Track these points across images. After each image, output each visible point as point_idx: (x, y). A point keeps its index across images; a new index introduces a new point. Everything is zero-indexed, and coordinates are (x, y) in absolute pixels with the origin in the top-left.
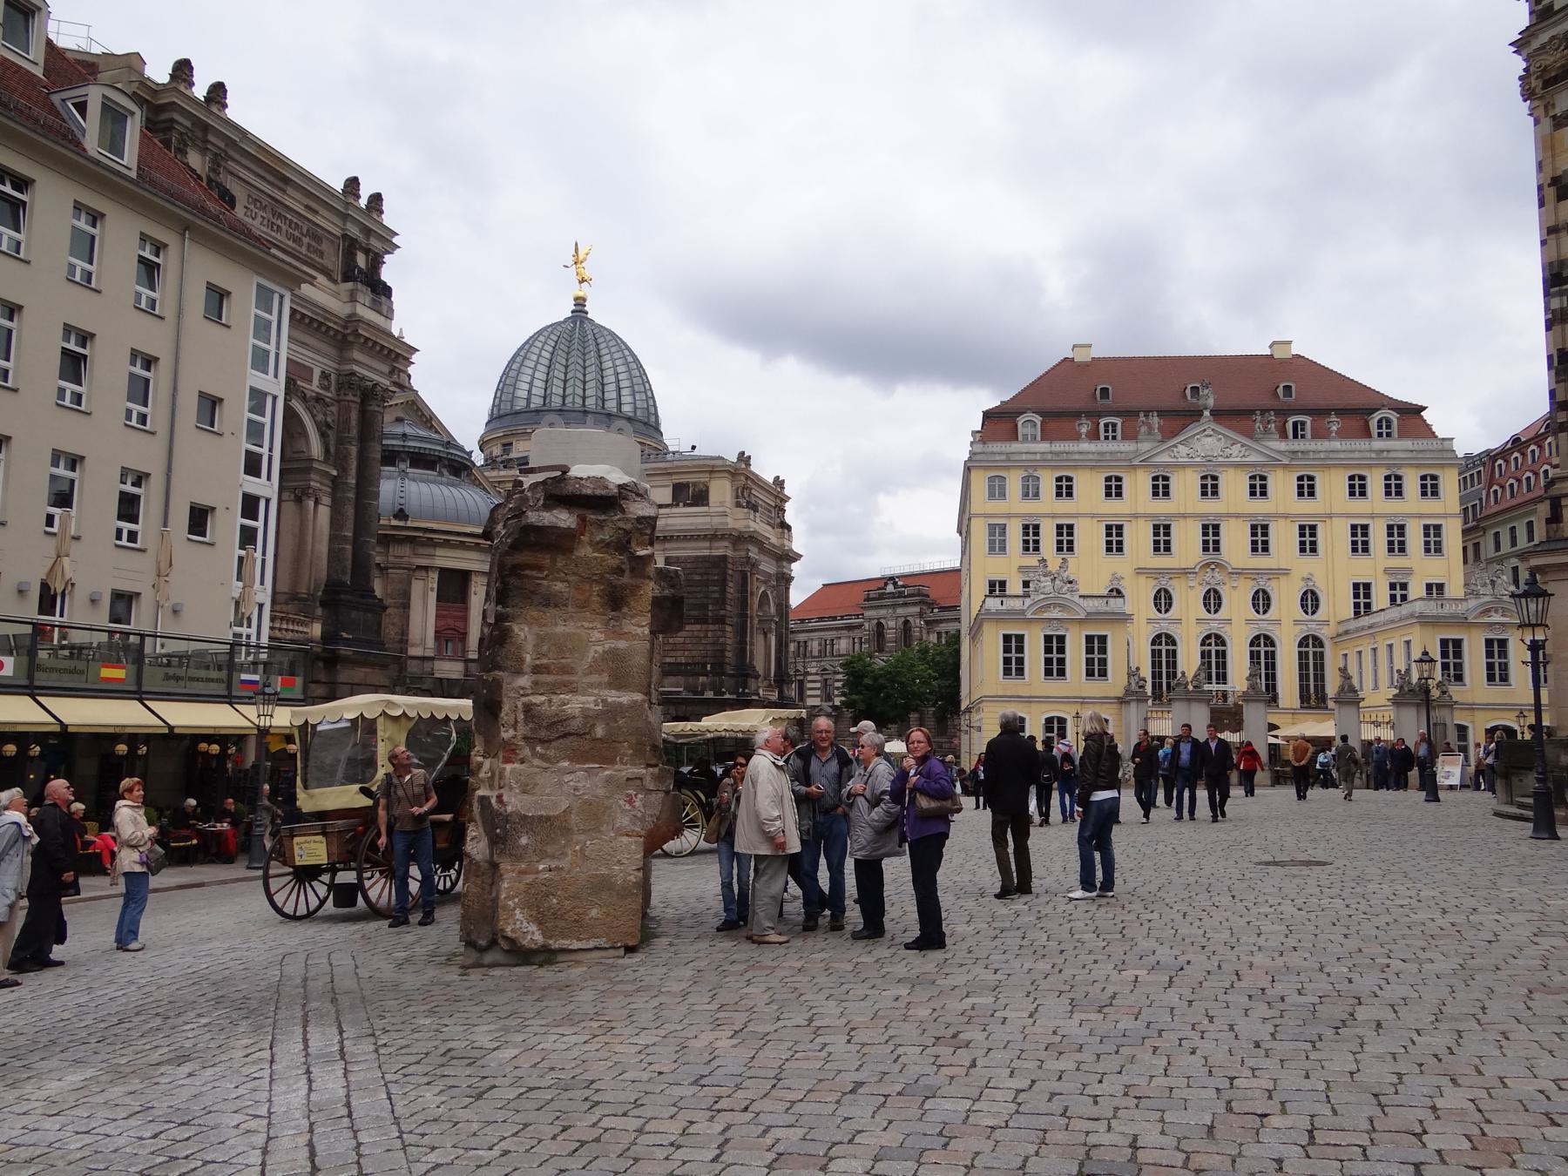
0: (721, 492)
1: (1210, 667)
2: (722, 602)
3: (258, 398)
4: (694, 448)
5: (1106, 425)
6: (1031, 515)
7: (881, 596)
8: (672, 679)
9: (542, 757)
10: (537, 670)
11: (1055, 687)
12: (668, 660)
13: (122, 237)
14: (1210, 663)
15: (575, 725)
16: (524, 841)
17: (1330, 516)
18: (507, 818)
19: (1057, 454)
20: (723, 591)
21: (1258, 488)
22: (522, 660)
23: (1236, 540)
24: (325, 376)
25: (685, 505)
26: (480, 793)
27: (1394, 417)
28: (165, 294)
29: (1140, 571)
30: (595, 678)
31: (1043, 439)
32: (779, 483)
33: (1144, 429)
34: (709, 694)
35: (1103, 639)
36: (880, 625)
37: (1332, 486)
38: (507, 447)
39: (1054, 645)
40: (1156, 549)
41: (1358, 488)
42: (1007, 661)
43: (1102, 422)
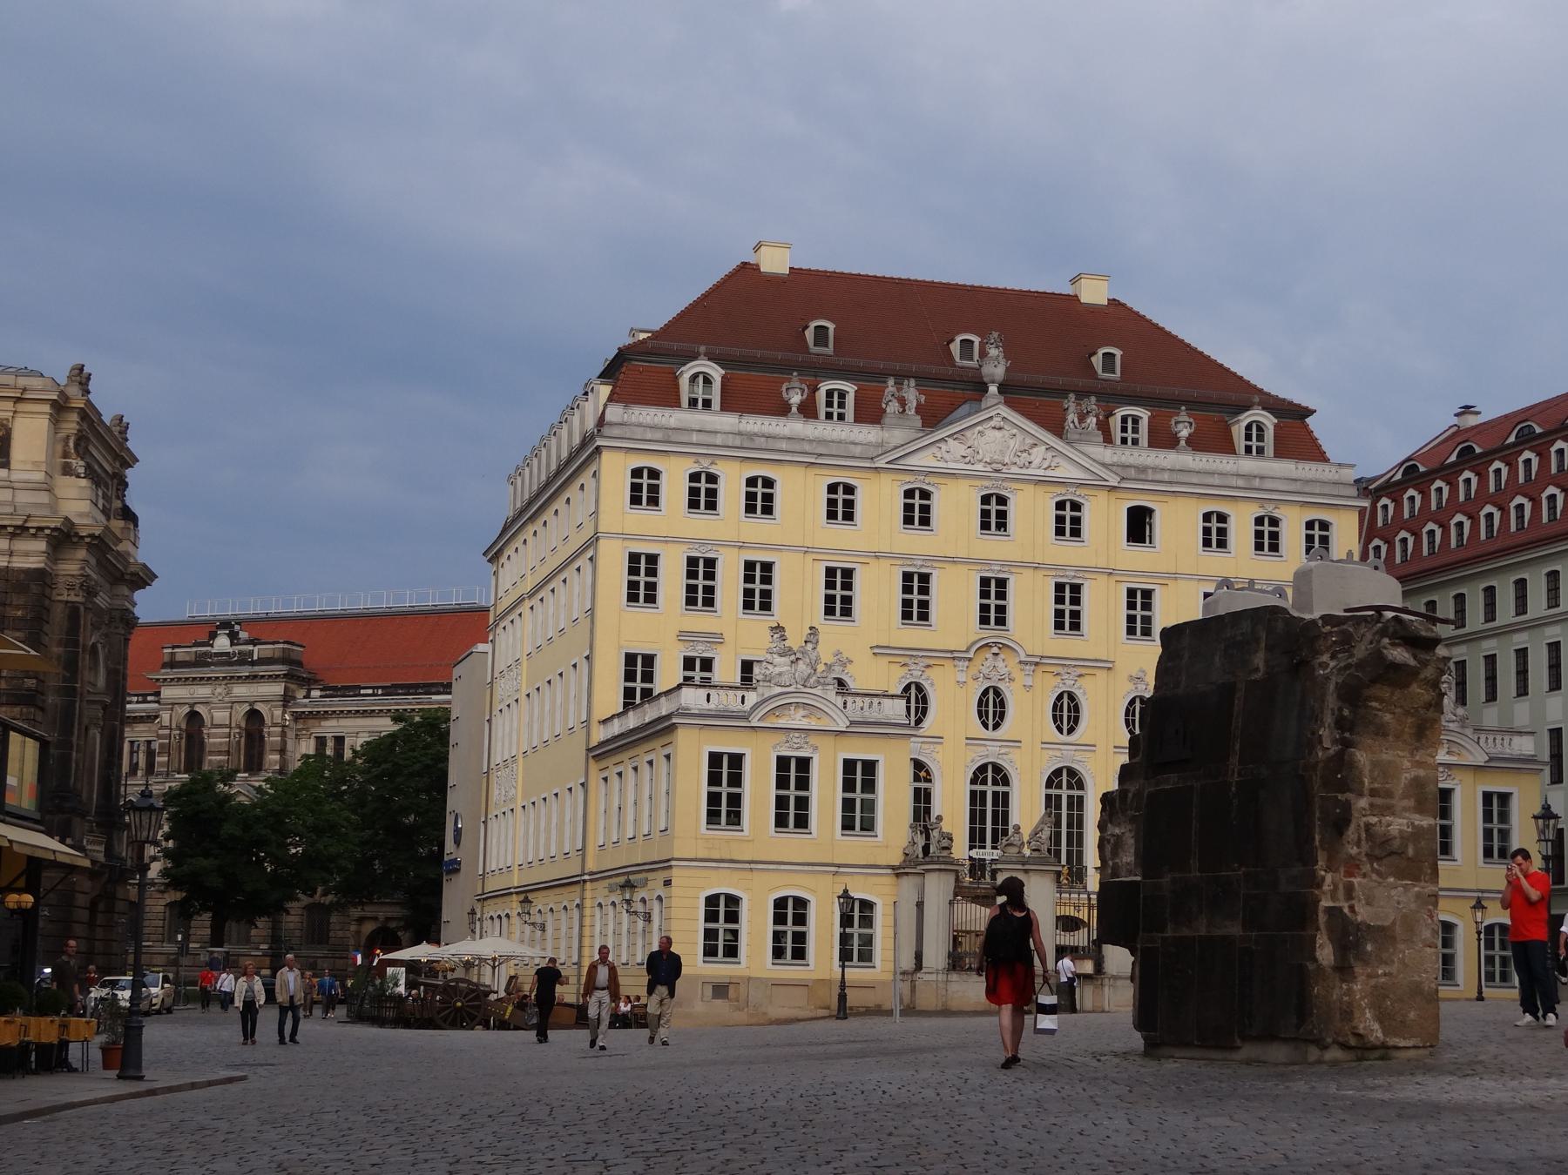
1: (1058, 824)
5: (830, 394)
6: (702, 542)
7: (200, 661)
9: (1379, 873)
10: (1374, 793)
11: (791, 844)
14: (1058, 817)
15: (1396, 843)
16: (1369, 948)
17: (1175, 576)
18: (1358, 926)
19: (751, 436)
21: (1068, 523)
22: (1362, 783)
23: (1030, 605)
26: (1325, 903)
27: (1269, 421)
29: (879, 651)
30: (1406, 803)
31: (726, 407)
32: (122, 425)
33: (893, 407)
35: (870, 767)
36: (194, 717)
37: (1177, 523)
39: (791, 773)
40: (907, 615)
41: (1215, 534)
42: (714, 799)
43: (825, 387)
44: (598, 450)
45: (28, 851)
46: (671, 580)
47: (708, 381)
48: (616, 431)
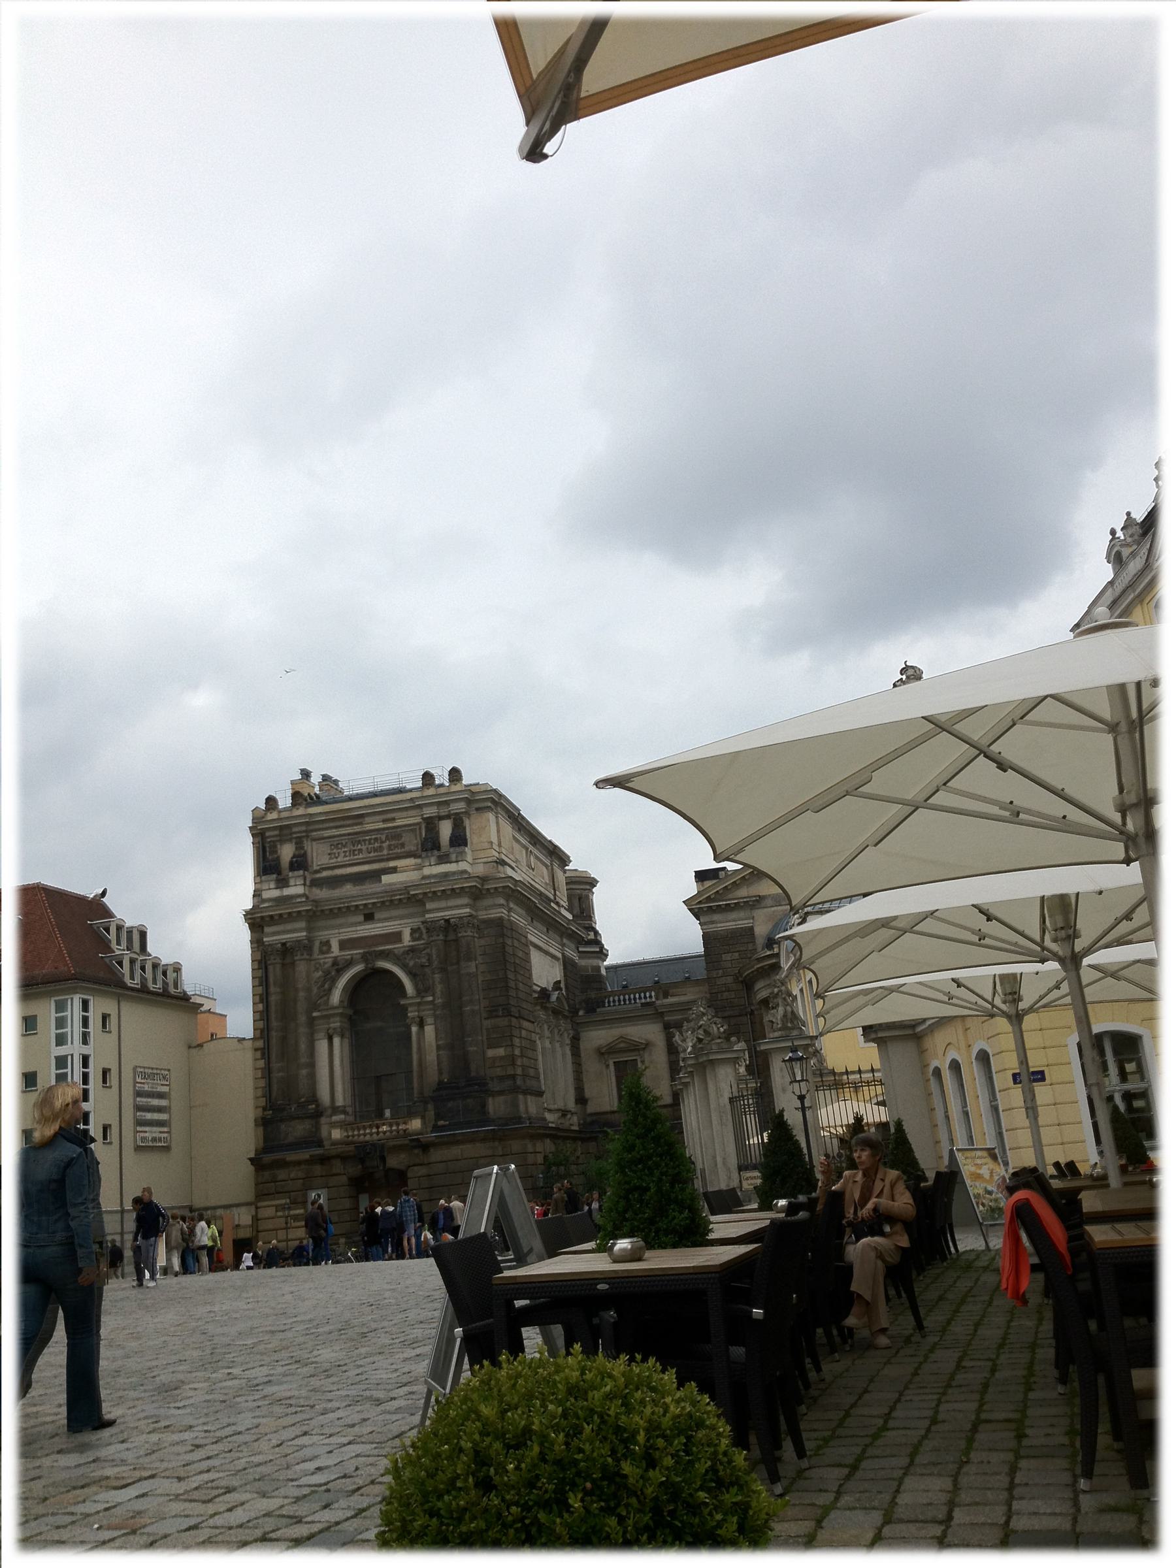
24: (413, 931)
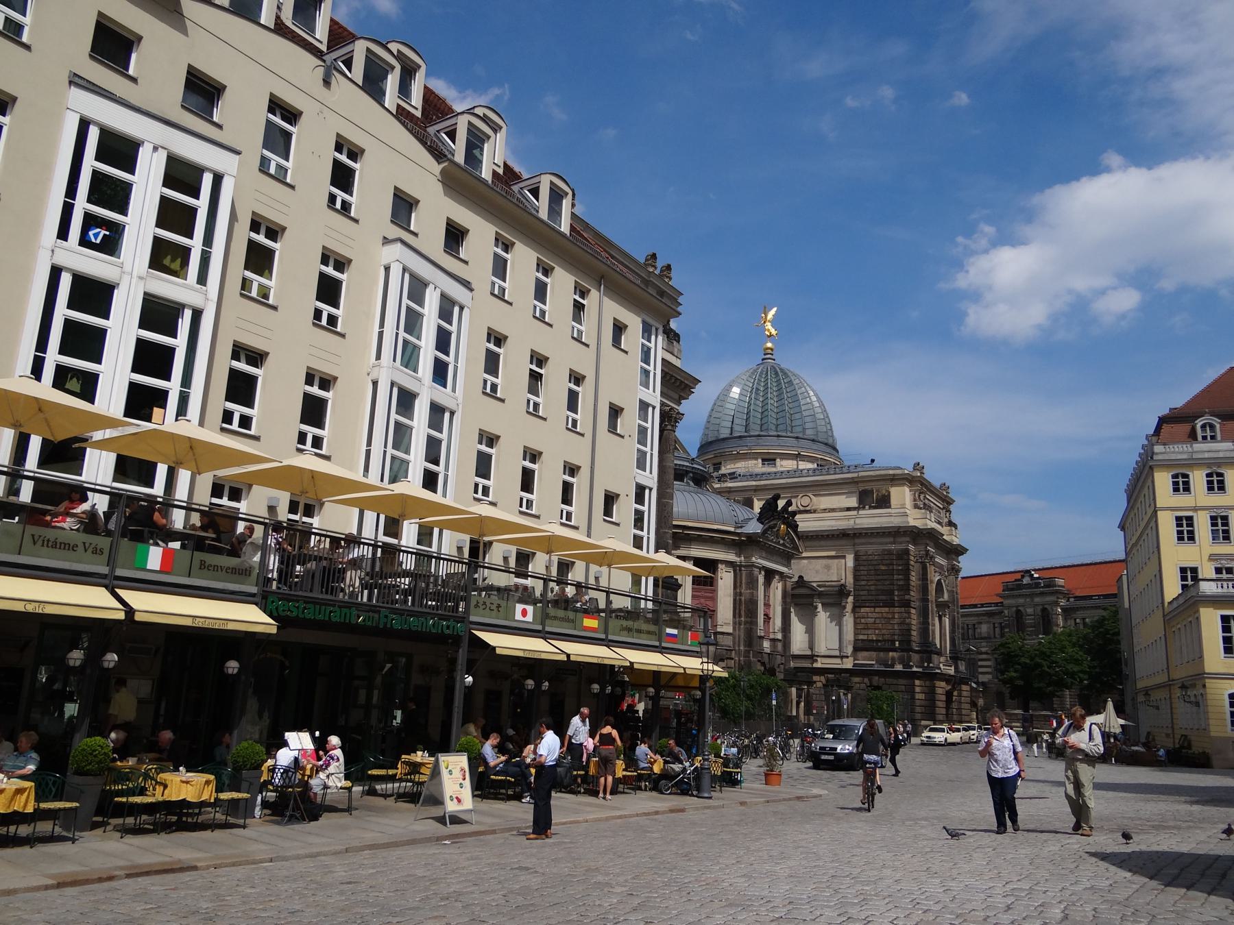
0: (902, 496)
2: (906, 588)
3: (644, 406)
4: (873, 461)
7: (1020, 587)
8: (865, 654)
12: (861, 637)
13: (562, 282)
20: (907, 579)
25: (871, 508)
28: (587, 328)
34: (899, 667)
36: (1018, 612)
38: (717, 467)
44: (1151, 468)
45: (655, 668)
46: (1203, 525)
47: (1212, 427)
48: (1160, 457)
